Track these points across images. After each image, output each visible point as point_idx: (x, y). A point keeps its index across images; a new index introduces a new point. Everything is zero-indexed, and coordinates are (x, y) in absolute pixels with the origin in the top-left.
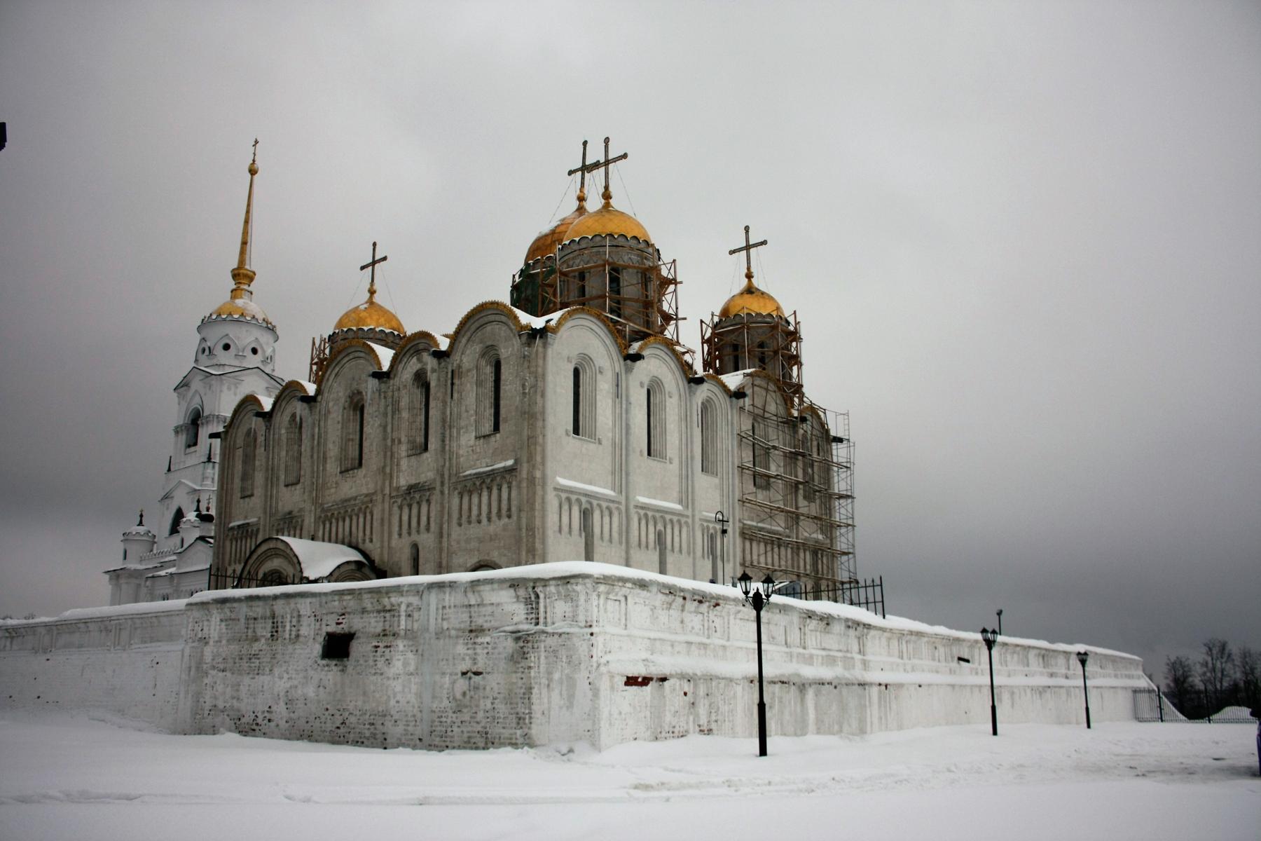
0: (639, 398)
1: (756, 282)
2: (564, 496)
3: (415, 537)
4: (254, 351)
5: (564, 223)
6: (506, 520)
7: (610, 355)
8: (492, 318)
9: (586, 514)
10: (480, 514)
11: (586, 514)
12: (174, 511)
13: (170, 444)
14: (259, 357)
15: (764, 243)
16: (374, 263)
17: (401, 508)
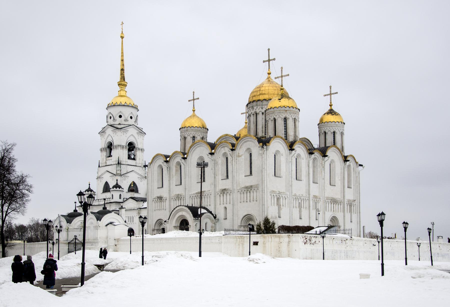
1: (333, 107)
3: (225, 205)
4: (131, 118)
5: (263, 84)
6: (255, 202)
7: (284, 148)
8: (250, 140)
9: (278, 199)
10: (247, 199)
11: (278, 199)
12: (104, 183)
13: (101, 156)
14: (134, 119)
15: (336, 93)
16: (194, 100)
17: (220, 196)
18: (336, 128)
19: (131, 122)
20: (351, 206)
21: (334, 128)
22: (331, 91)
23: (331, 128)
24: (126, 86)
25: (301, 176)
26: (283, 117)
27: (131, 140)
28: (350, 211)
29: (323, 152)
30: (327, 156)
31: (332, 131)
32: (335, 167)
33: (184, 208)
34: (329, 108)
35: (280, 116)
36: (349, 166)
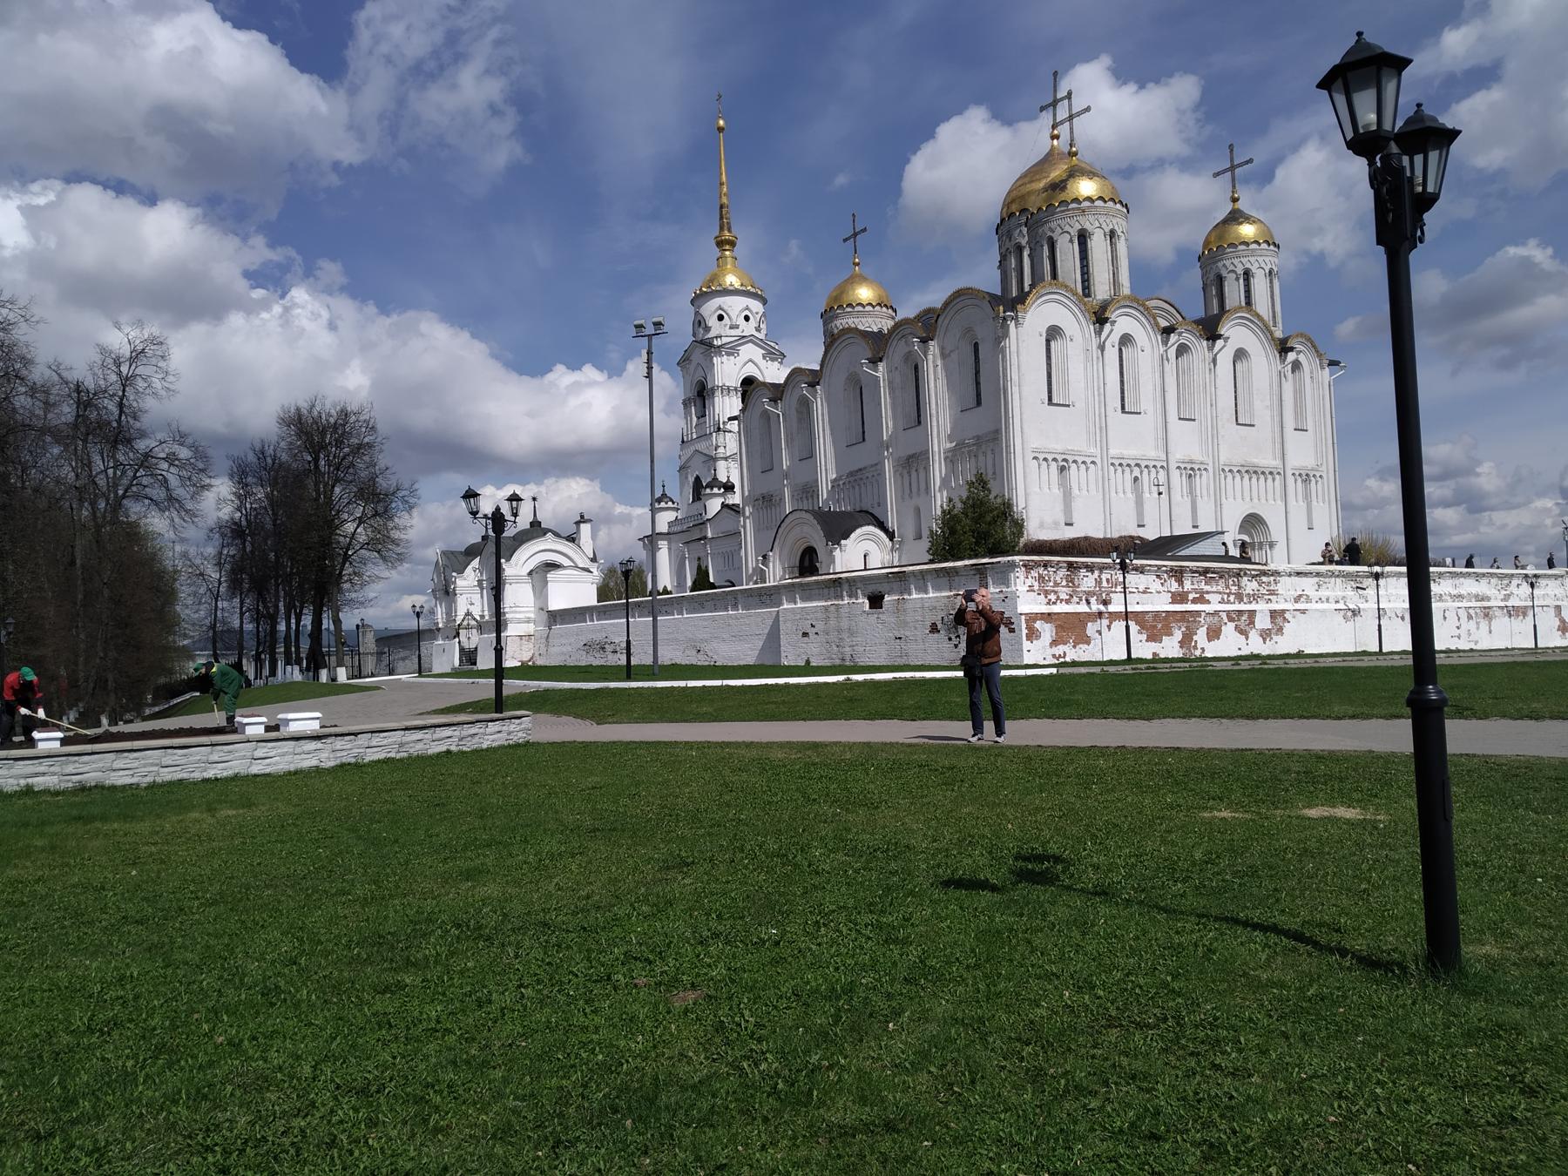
0: (1112, 353)
2: (1041, 457)
4: (747, 318)
9: (1062, 469)
18: (1252, 259)
19: (748, 329)
20: (1307, 479)
21: (1244, 260)
22: (1232, 160)
23: (1236, 261)
24: (732, 244)
25: (1137, 401)
26: (1074, 232)
27: (750, 370)
28: (1307, 497)
29: (1210, 330)
30: (1220, 337)
31: (1240, 271)
32: (1249, 371)
33: (804, 515)
34: (1229, 207)
35: (1067, 228)
36: (1296, 366)
